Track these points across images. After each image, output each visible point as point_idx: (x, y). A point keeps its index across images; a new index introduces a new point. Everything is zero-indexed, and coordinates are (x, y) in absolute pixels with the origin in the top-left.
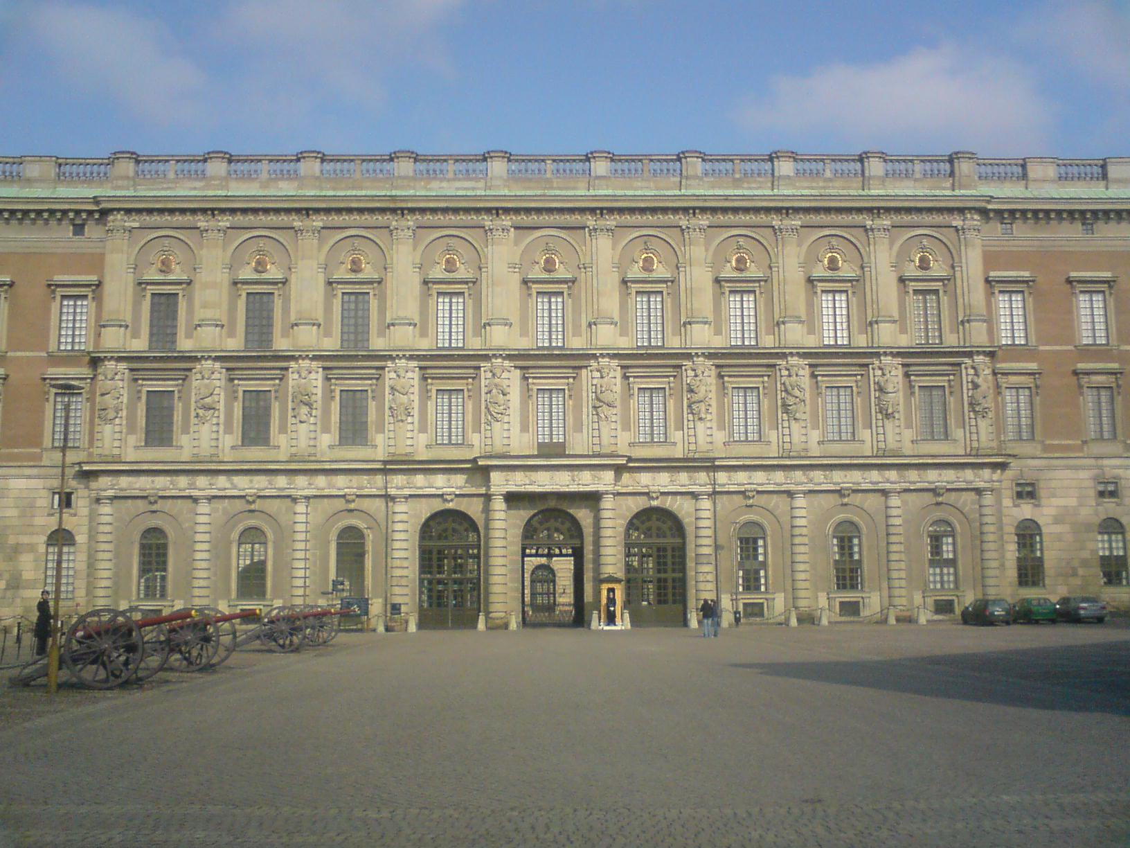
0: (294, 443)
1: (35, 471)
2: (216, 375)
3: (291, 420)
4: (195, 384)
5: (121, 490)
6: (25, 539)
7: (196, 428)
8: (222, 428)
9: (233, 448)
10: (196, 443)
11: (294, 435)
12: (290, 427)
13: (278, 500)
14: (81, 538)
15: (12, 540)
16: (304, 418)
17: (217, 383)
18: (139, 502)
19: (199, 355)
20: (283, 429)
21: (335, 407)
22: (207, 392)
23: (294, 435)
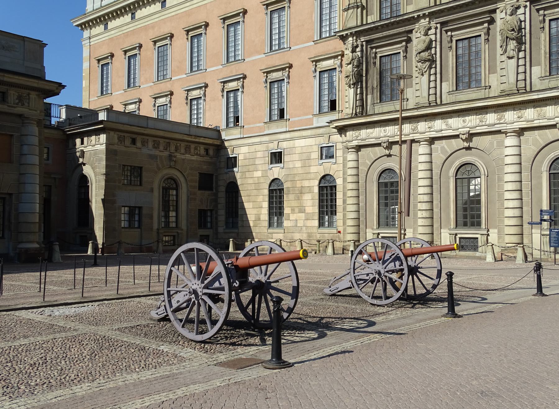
0: (504, 79)
1: (308, 133)
2: (433, 31)
3: (499, 58)
4: (415, 41)
5: (362, 140)
6: (306, 183)
7: (417, 80)
8: (438, 76)
9: (449, 93)
10: (418, 94)
11: (504, 72)
12: (499, 66)
13: (489, 137)
14: (339, 182)
15: (298, 184)
16: (511, 53)
17: (433, 37)
18: (377, 149)
19: (415, 15)
20: (492, 70)
21: (544, 37)
22: (422, 46)
23: (504, 72)
